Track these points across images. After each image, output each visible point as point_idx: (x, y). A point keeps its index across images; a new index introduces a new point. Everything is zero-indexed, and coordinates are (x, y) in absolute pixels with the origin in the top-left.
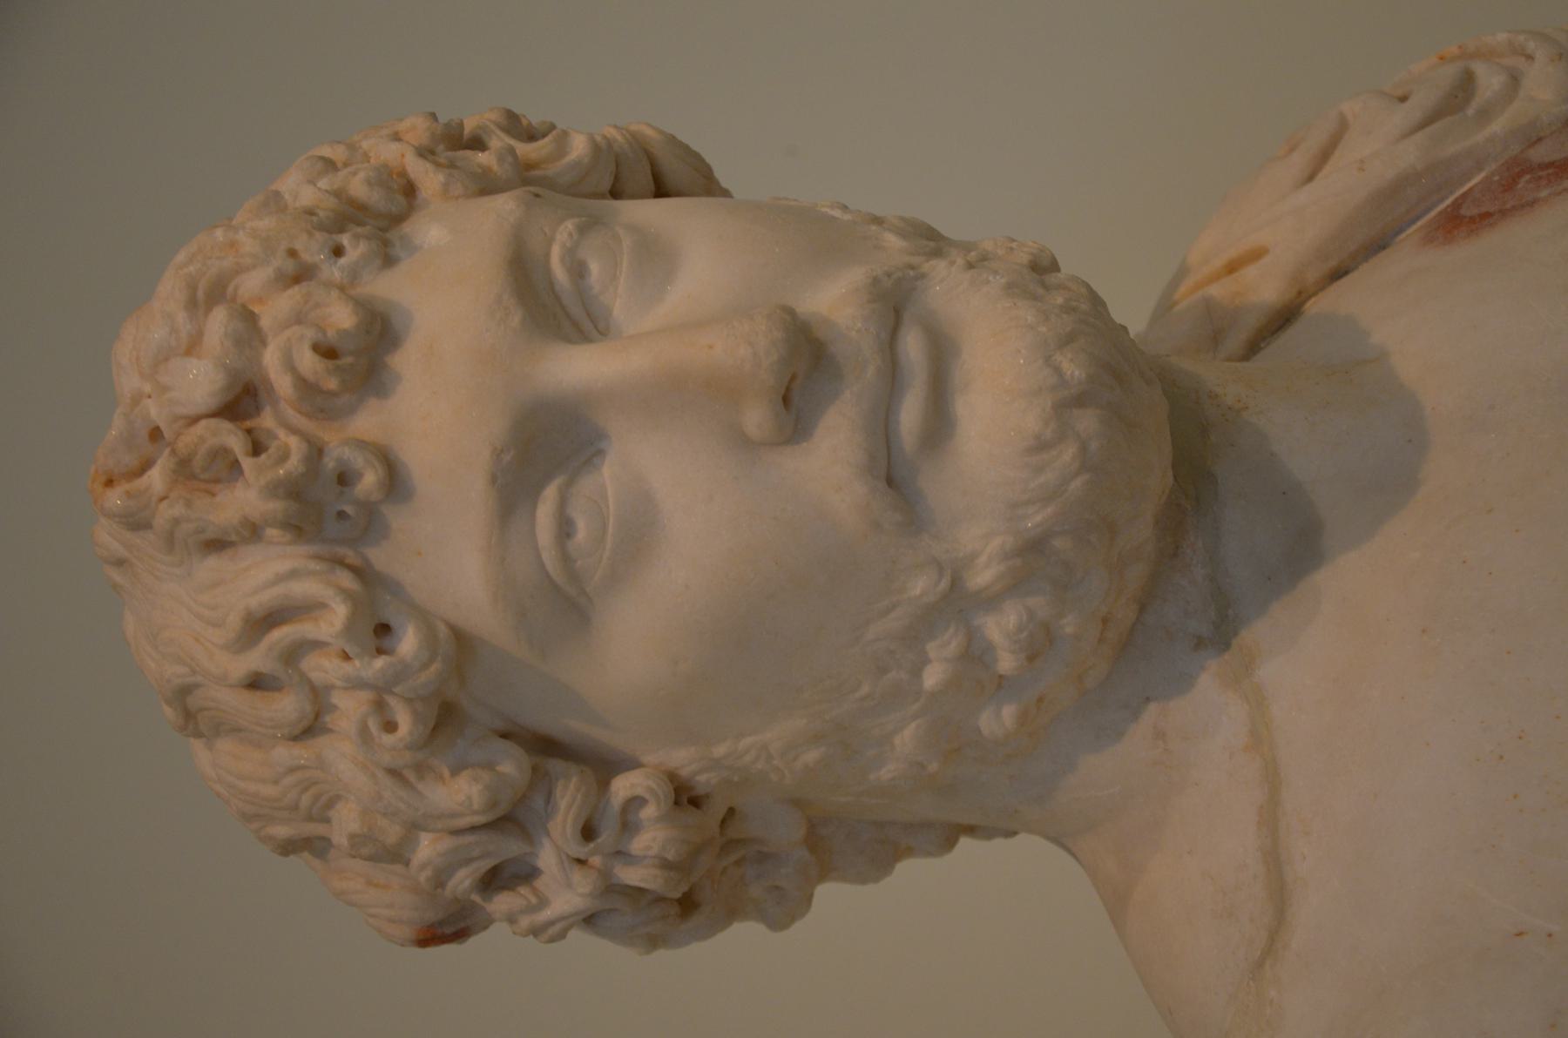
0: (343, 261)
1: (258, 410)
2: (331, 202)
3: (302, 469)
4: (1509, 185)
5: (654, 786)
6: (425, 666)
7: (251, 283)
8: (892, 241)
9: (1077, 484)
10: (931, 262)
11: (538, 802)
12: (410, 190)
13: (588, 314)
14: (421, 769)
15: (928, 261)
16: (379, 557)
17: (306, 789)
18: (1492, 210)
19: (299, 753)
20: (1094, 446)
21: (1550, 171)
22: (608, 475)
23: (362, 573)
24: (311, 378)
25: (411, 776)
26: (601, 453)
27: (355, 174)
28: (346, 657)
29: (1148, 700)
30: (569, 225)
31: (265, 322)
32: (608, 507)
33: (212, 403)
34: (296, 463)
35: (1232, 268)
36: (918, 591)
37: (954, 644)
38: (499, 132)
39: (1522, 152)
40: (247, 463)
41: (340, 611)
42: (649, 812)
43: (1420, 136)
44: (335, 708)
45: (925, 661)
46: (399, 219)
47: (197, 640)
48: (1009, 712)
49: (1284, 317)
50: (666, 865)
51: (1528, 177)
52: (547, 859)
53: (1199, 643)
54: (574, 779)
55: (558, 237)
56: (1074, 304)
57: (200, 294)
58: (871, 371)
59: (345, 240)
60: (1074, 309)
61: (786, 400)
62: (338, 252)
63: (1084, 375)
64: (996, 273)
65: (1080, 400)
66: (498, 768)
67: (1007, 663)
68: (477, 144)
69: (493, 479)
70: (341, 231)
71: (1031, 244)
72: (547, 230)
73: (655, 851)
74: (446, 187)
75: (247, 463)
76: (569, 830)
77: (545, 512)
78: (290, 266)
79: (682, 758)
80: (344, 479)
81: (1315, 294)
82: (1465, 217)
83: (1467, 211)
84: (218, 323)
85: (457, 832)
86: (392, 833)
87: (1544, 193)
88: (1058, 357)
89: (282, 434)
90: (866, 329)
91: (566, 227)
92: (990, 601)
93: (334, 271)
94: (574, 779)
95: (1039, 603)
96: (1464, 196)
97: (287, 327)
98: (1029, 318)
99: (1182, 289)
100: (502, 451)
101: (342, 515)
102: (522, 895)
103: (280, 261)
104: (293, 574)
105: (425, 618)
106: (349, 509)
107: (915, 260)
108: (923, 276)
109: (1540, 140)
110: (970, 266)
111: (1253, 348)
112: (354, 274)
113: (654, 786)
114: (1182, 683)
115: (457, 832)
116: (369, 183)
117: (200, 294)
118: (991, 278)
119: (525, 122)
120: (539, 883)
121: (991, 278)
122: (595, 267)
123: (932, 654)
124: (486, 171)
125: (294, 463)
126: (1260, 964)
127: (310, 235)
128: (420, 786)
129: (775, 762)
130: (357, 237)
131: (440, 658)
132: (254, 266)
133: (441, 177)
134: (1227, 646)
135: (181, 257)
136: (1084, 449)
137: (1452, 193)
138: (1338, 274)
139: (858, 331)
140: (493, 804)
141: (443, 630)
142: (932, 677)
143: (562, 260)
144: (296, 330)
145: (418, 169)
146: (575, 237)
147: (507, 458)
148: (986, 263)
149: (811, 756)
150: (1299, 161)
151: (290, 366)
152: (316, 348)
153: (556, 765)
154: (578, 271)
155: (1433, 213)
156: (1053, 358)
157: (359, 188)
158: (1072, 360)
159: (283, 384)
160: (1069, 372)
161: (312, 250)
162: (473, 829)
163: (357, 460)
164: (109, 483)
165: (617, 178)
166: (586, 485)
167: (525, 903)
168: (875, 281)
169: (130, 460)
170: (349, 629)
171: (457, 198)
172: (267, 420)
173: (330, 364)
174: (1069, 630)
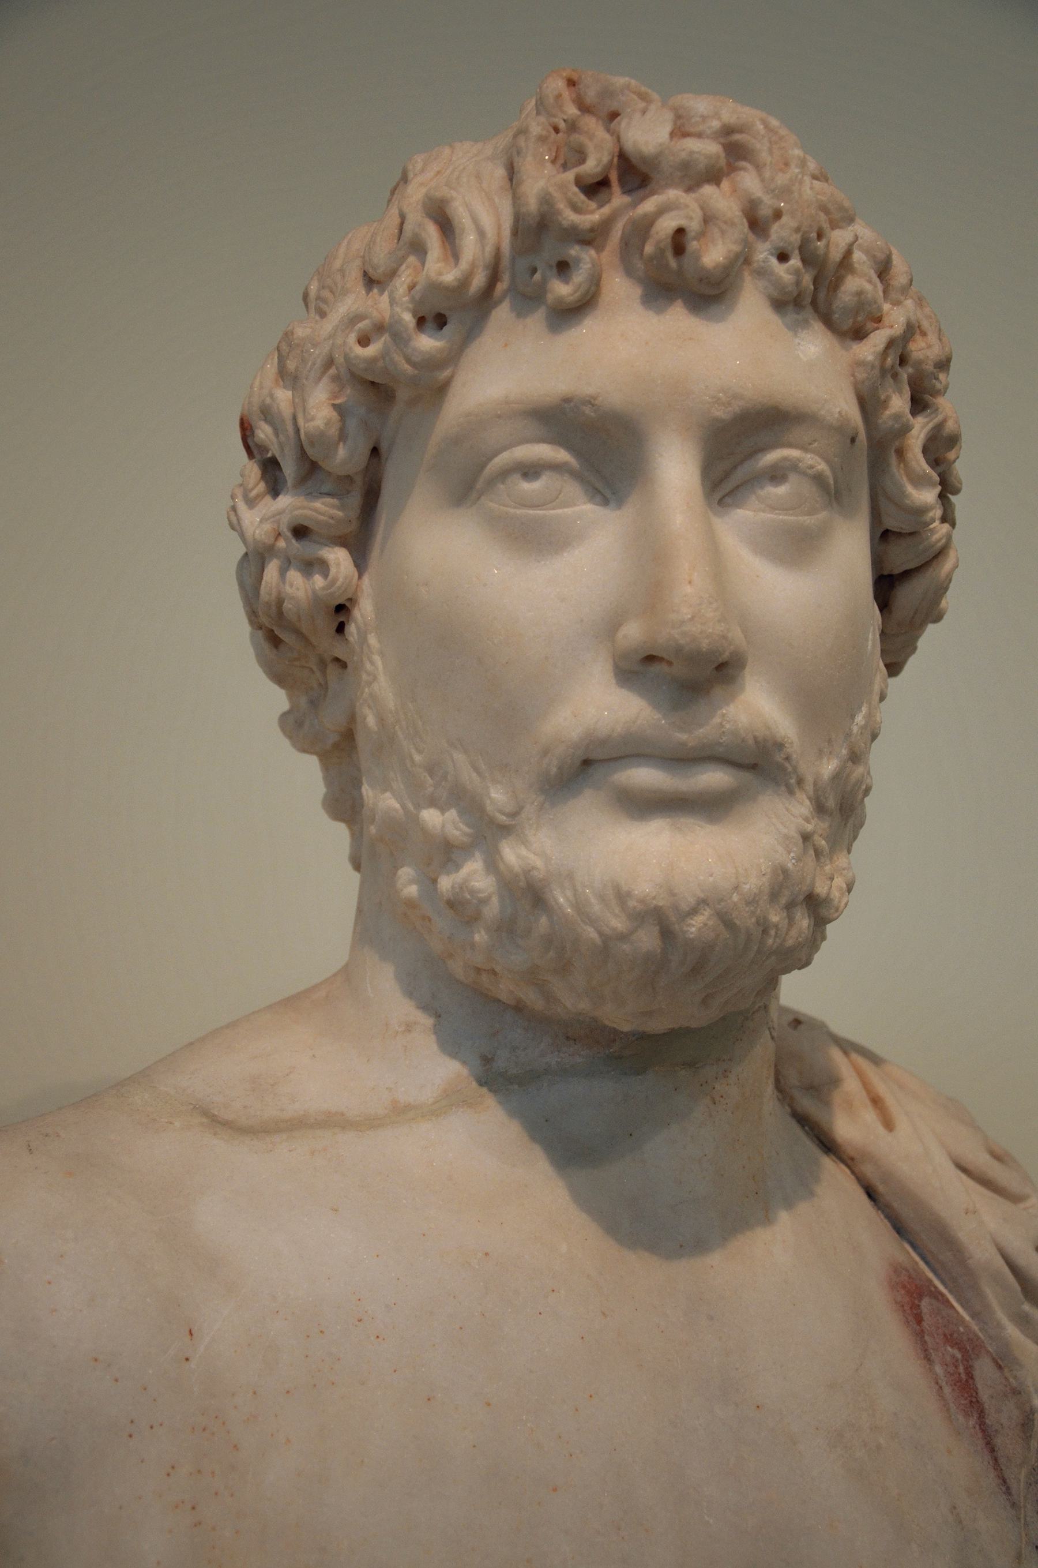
0: (774, 261)
1: (627, 192)
2: (836, 255)
3: (565, 223)
4: (950, 1339)
5: (339, 583)
6: (409, 361)
7: (749, 181)
8: (829, 767)
9: (591, 933)
10: (807, 802)
11: (327, 487)
12: (859, 334)
13: (738, 487)
14: (336, 379)
15: (809, 798)
16: (502, 313)
17: (332, 291)
18: (925, 1324)
19: (354, 274)
20: (626, 947)
21: (963, 1376)
22: (587, 509)
23: (487, 298)
24: (654, 230)
25: (332, 371)
26: (605, 502)
27: (870, 281)
28: (411, 287)
29: (439, 1016)
30: (822, 466)
31: (708, 190)
32: (554, 509)
33: (629, 146)
35: (876, 1101)
36: (493, 795)
37: (457, 833)
38: (931, 425)
39: (988, 1352)
40: (570, 175)
41: (450, 277)
42: (319, 581)
43: (1000, 1262)
44: (382, 292)
45: (443, 811)
46: (828, 321)
47: (439, 172)
48: (413, 890)
49: (828, 1145)
50: (280, 602)
51: (959, 1356)
52: (284, 501)
53: (487, 1060)
56: (773, 932)
57: (737, 137)
58: (683, 737)
59: (795, 262)
60: (765, 932)
61: (650, 659)
62: (783, 257)
63: (692, 936)
64: (799, 859)
65: (667, 933)
66: (341, 445)
67: (446, 883)
68: (919, 404)
69: (567, 400)
70: (804, 261)
71: (844, 900)
72: (816, 444)
73: (288, 589)
74: (860, 364)
75: (570, 175)
76: (296, 513)
77: (545, 451)
78: (765, 211)
79: (365, 610)
80: (563, 268)
81: (853, 1172)
82: (920, 1301)
83: (926, 1304)
84: (707, 149)
85: (295, 418)
86: (291, 365)
87: (938, 1369)
89: (606, 210)
90: (723, 732)
91: (820, 464)
92: (492, 865)
93: (763, 253)
94: (340, 514)
95: (493, 910)
96: (948, 1301)
97: (702, 208)
99: (861, 1061)
100: (593, 405)
101: (534, 271)
102: (257, 484)
103: (768, 203)
104: (481, 234)
105: (452, 358)
106: (538, 276)
107: (809, 787)
108: (791, 792)
109: (1000, 1367)
110: (806, 837)
111: (803, 1120)
112: (762, 273)
113: (339, 583)
115: (295, 418)
116: (860, 293)
117: (737, 137)
118: (792, 855)
119: (951, 455)
120: (268, 499)
121: (792, 855)
122: (782, 490)
123: (447, 814)
124: (885, 404)
125: (570, 217)
126: (205, 1113)
127: (797, 230)
128: (325, 380)
129: (367, 690)
130: (797, 272)
131: (416, 372)
132: (763, 180)
133: (870, 358)
134: (481, 1084)
135: (774, 122)
136: (623, 937)
137: (950, 1291)
138: (871, 1193)
139: (721, 725)
140: (312, 444)
142: (431, 817)
144: (697, 215)
145: (878, 340)
146: (810, 472)
147: (587, 410)
148: (812, 852)
149: (371, 721)
150: (982, 1160)
151: (661, 211)
152: (680, 231)
153: (355, 500)
154: (776, 475)
155: (931, 1275)
156: (706, 907)
157: (852, 284)
158: (705, 925)
159: (649, 206)
160: (693, 922)
161: (782, 232)
162: (297, 431)
163: (580, 276)
164: (571, 83)
165: (899, 535)
166: (572, 489)
167: (250, 486)
168: (780, 746)
169: (591, 95)
170: (435, 287)
171: (853, 375)
172: (618, 199)
173: (668, 242)
174: (477, 937)
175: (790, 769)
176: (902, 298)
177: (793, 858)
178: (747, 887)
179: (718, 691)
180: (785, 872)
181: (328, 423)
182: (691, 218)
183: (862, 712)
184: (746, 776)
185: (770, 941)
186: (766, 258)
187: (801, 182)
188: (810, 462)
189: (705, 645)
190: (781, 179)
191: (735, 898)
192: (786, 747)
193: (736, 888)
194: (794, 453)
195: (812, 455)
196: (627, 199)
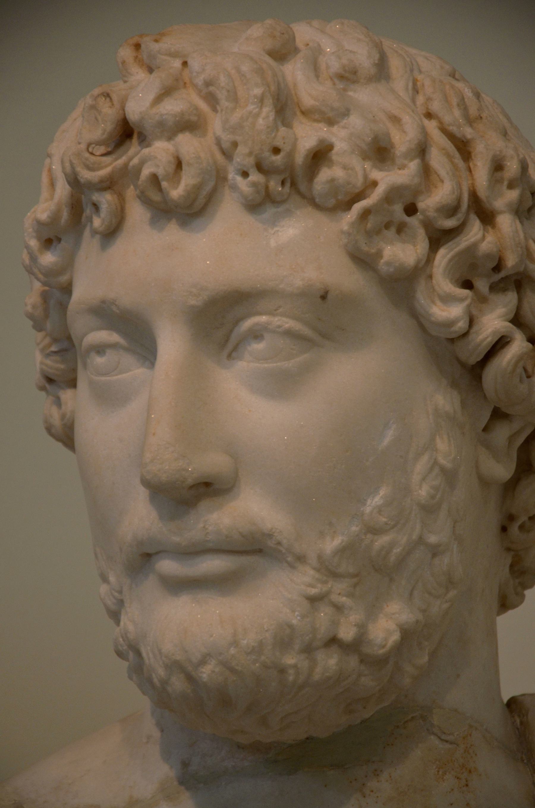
10: (312, 572)
32: (117, 375)
34: (86, 176)
38: (449, 256)
54: (62, 366)
55: (276, 319)
56: (291, 671)
58: (176, 539)
62: (245, 174)
64: (303, 616)
65: (190, 678)
69: (103, 302)
72: (281, 310)
74: (342, 232)
78: (226, 145)
88: (213, 662)
94: (62, 366)
98: (245, 642)
108: (292, 566)
114: (166, 755)
117: (211, 88)
118: (297, 613)
121: (297, 613)
122: (258, 347)
124: (379, 254)
127: (250, 154)
141: (64, 279)
143: (257, 324)
146: (280, 330)
147: (114, 309)
158: (213, 672)
160: (204, 670)
166: (128, 359)
168: (270, 536)
170: (39, 223)
175: (284, 551)
176: (406, 162)
177: (298, 615)
178: (245, 642)
179: (204, 505)
180: (291, 626)
181: (34, 307)
182: (158, 166)
183: (379, 494)
184: (244, 560)
185: (291, 678)
186: (234, 177)
187: (257, 115)
188: (278, 323)
189: (164, 478)
190: (236, 117)
191: (233, 651)
192: (274, 536)
193: (235, 643)
194: (264, 319)
195: (280, 318)
196: (139, 148)
